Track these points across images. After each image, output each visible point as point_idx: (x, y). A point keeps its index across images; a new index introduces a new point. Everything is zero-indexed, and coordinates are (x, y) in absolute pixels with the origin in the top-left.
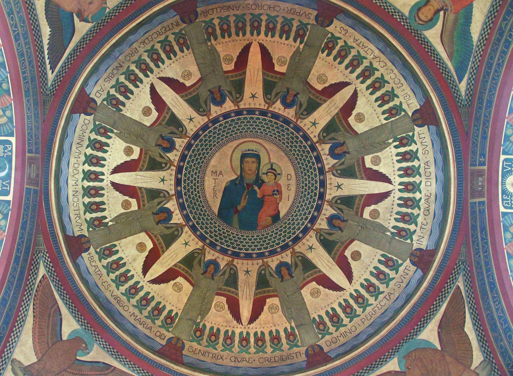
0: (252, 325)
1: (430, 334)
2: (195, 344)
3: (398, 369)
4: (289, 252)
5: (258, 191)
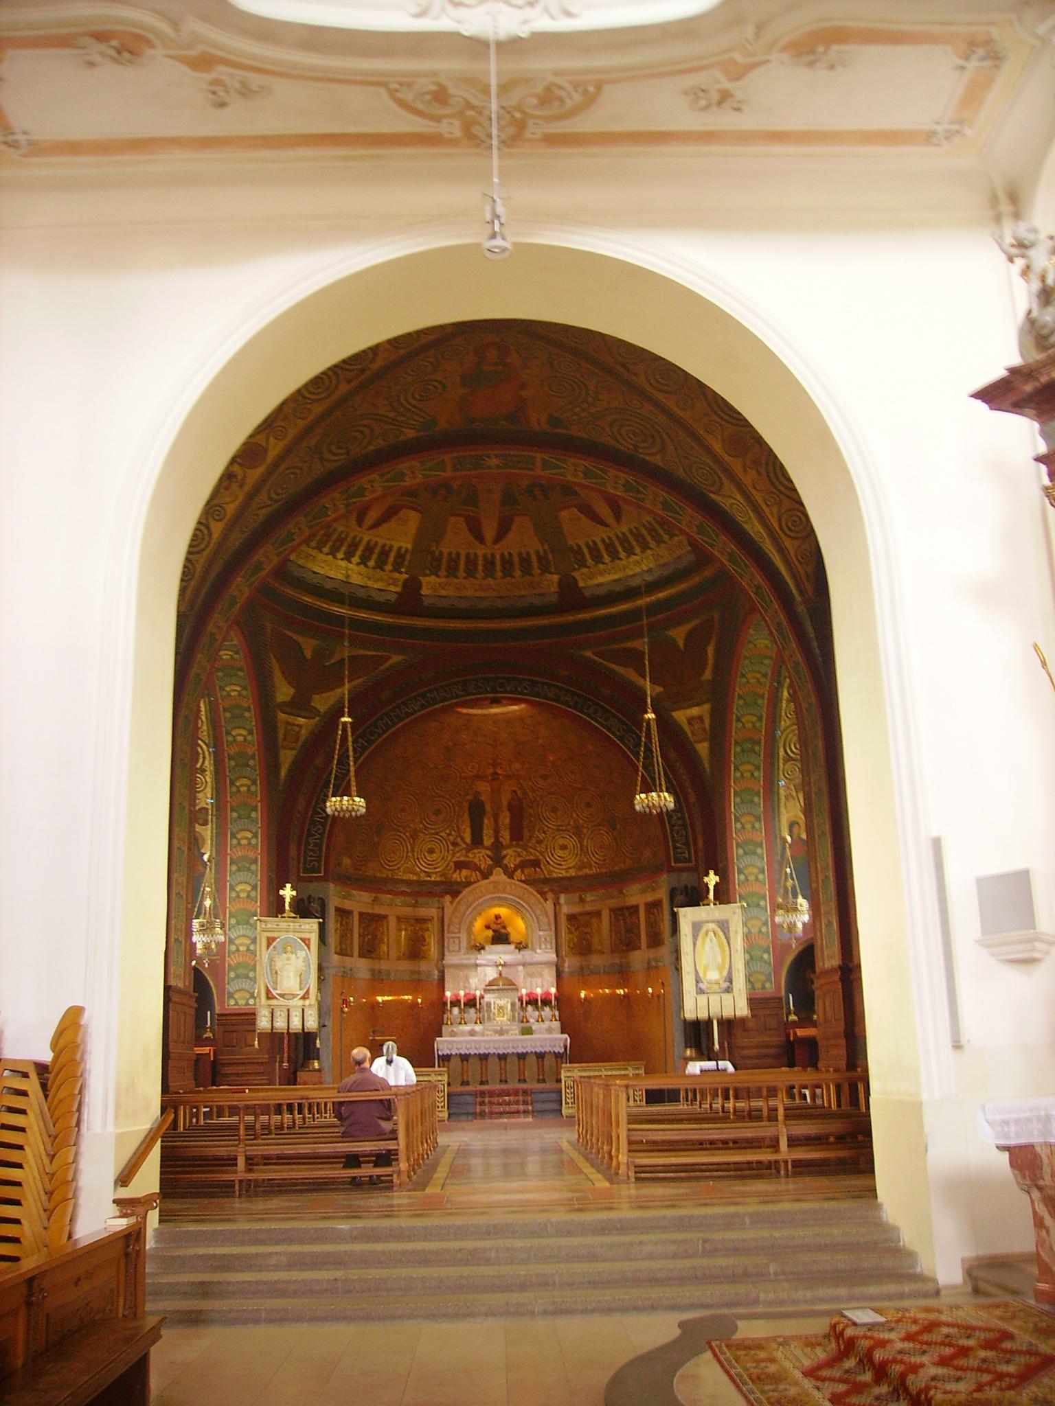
0: (496, 547)
1: (678, 634)
2: (433, 579)
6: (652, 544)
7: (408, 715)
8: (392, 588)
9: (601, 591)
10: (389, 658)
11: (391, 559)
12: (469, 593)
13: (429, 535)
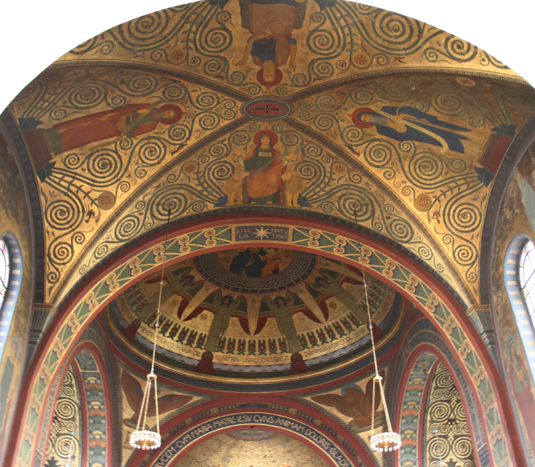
0: (256, 336)
2: (219, 353)
3: (340, 394)
4: (284, 291)
5: (262, 258)
6: (346, 332)
7: (201, 434)
8: (196, 357)
9: (316, 362)
10: (192, 398)
11: (196, 341)
12: (240, 363)
13: (219, 326)
